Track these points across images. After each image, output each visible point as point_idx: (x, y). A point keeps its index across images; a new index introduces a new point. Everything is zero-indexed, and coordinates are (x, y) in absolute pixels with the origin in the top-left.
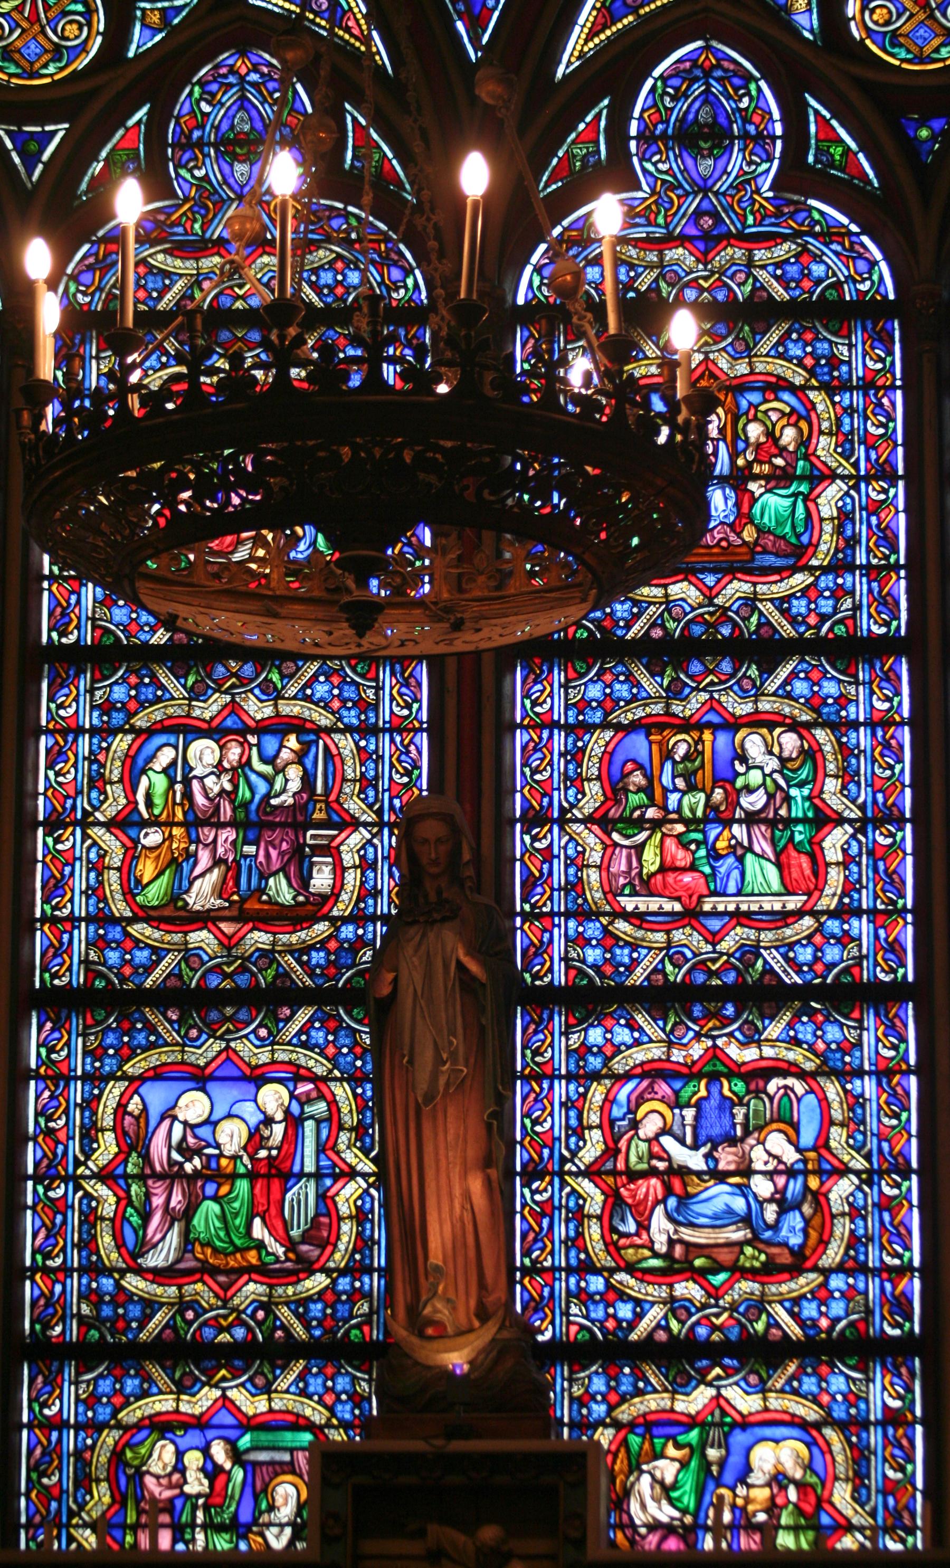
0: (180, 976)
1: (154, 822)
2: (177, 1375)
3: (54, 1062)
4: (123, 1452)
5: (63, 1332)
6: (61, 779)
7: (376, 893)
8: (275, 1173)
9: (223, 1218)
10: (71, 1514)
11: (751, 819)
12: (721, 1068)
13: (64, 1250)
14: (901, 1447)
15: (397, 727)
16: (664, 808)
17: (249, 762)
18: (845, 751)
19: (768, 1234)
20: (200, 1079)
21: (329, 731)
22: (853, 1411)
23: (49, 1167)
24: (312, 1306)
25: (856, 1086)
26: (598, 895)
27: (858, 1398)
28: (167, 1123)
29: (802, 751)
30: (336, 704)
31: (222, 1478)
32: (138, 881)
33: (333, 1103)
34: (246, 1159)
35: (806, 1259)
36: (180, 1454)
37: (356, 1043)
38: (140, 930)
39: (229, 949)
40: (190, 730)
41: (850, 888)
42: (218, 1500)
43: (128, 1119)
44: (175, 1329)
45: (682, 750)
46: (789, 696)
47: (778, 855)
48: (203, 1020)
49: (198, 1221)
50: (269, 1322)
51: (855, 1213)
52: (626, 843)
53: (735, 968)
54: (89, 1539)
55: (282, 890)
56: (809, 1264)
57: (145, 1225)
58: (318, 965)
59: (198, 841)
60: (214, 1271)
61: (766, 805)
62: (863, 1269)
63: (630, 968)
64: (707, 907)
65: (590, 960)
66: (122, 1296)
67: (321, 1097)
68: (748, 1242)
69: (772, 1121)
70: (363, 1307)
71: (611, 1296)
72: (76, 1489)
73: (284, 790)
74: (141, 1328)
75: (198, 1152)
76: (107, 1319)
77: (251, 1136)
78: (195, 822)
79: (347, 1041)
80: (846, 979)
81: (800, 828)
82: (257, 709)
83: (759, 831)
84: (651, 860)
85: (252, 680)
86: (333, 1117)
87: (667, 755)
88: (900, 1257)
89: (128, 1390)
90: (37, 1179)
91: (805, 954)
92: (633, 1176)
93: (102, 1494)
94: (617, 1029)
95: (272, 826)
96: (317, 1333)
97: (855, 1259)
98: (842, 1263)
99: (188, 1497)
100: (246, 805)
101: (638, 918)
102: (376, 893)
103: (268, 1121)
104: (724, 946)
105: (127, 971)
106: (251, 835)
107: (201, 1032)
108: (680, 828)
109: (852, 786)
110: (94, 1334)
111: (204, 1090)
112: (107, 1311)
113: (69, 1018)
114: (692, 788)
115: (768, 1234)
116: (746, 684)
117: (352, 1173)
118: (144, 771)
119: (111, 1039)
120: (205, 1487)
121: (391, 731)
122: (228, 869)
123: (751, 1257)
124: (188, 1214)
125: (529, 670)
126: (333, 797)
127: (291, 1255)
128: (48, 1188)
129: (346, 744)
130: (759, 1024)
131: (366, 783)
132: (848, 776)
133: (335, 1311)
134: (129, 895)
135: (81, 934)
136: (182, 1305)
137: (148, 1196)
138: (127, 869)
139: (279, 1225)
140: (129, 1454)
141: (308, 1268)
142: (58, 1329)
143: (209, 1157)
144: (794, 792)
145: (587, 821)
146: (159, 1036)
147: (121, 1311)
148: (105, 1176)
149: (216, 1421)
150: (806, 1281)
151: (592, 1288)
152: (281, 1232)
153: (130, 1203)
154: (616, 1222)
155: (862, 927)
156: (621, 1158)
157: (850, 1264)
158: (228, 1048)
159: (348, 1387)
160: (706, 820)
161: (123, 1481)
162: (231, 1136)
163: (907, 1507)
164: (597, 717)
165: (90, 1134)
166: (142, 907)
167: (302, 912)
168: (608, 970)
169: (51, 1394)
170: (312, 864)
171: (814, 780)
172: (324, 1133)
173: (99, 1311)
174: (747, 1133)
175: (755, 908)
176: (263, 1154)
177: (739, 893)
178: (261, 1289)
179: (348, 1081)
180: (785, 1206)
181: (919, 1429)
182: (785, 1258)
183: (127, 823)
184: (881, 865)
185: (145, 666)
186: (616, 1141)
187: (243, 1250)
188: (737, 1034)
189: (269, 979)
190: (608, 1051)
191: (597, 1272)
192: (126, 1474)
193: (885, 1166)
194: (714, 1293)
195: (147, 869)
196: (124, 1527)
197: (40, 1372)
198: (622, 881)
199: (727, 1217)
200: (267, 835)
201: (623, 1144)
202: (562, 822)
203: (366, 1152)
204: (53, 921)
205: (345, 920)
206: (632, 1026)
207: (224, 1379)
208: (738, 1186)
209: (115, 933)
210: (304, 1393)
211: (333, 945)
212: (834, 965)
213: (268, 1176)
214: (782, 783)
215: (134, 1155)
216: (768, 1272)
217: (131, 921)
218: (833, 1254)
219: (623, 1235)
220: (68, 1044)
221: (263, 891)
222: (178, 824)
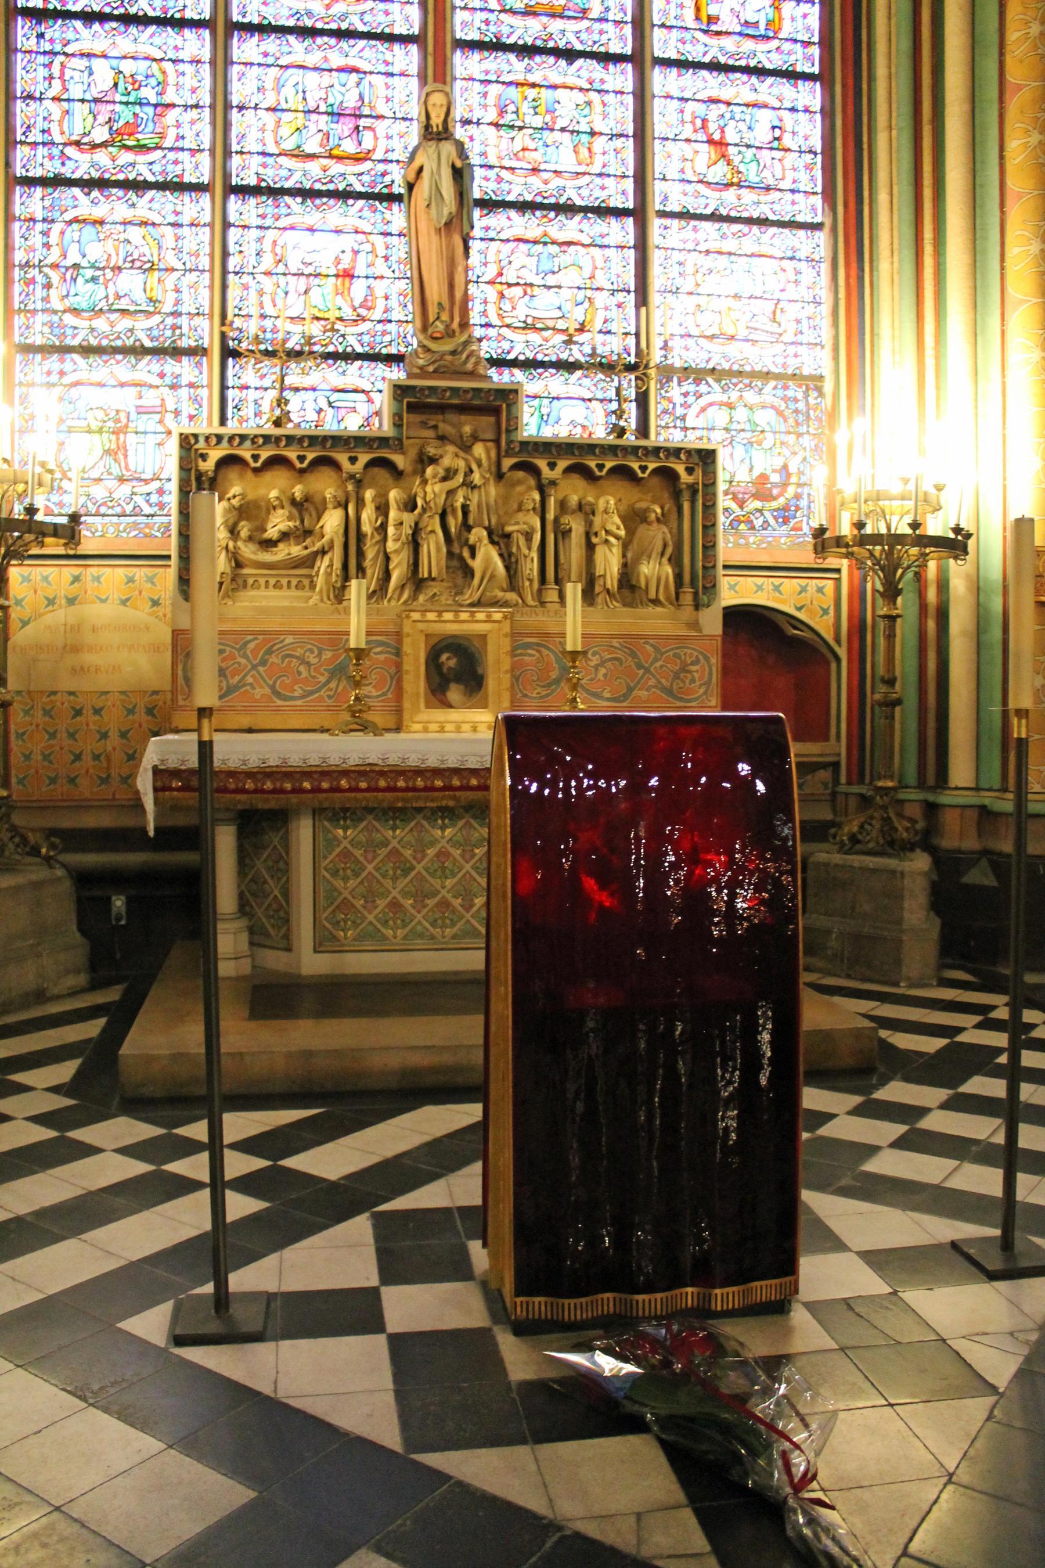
11: (563, 130)
38: (282, 160)
55: (349, 147)
70: (387, 338)
84: (517, 146)
92: (509, 285)
155: (609, 182)
164: (494, 78)
195: (285, 131)
209: (270, 160)
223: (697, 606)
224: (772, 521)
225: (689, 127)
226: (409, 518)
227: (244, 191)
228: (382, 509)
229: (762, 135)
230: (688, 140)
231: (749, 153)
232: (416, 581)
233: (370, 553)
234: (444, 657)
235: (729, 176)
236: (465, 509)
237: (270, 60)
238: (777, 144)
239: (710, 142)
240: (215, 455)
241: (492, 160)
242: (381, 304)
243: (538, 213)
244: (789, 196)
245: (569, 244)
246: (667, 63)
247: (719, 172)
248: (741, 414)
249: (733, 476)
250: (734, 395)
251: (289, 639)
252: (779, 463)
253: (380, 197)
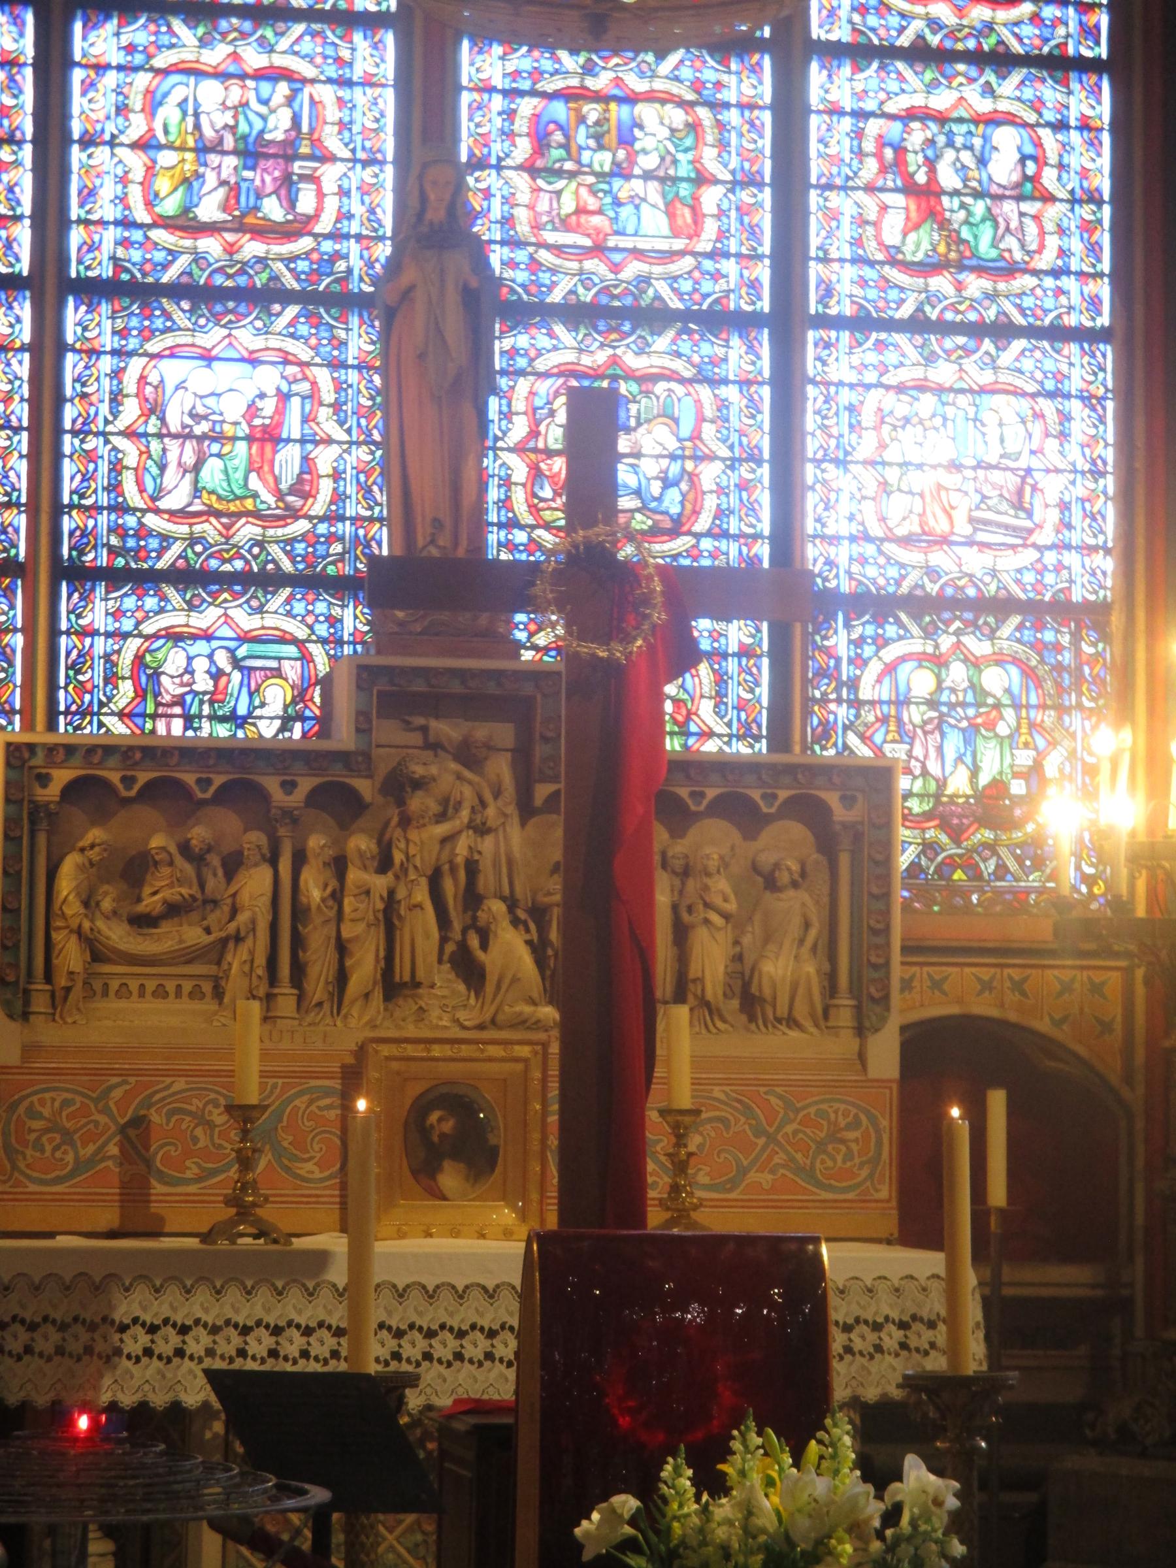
0: (190, 274)
1: (170, 147)
2: (188, 596)
3: (88, 339)
4: (143, 656)
5: (95, 558)
6: (92, 106)
7: (350, 217)
9: (226, 472)
10: (101, 704)
11: (647, 176)
12: (619, 372)
13: (95, 491)
14: (751, 674)
15: (368, 82)
16: (579, 162)
17: (247, 104)
18: (721, 126)
19: (653, 505)
20: (208, 358)
21: (313, 81)
22: (716, 645)
23: (84, 424)
24: (297, 545)
25: (723, 391)
26: (527, 229)
27: (720, 635)
28: (181, 391)
29: (687, 125)
30: (319, 60)
31: (224, 680)
32: (156, 195)
33: (314, 384)
34: (244, 426)
35: (683, 525)
36: (190, 659)
37: (334, 337)
38: (158, 235)
39: (231, 254)
40: (198, 73)
41: (722, 235)
42: (220, 697)
43: (149, 390)
44: (186, 558)
45: (592, 118)
46: (677, 79)
47: (667, 205)
48: (210, 311)
49: (205, 473)
50: (262, 557)
51: (721, 491)
52: (549, 188)
53: (632, 294)
54: (118, 727)
55: (273, 209)
56: (685, 528)
57: (162, 474)
58: (303, 272)
59: (206, 165)
60: (218, 514)
61: (659, 167)
62: (725, 534)
63: (551, 288)
64: (611, 243)
65: (519, 280)
66: (142, 532)
67: (305, 378)
68: (638, 510)
69: (659, 416)
70: (337, 548)
71: (533, 546)
72: (106, 685)
73: (276, 128)
74: (159, 557)
75: (205, 417)
76: (131, 550)
77: (249, 406)
78: (203, 149)
79: (326, 335)
80: (718, 308)
81: (684, 185)
82: (254, 59)
83: (653, 185)
84: (568, 205)
85: (251, 35)
86: (314, 395)
87: (582, 119)
88: (753, 526)
89: (147, 608)
90: (75, 433)
91: (686, 286)
93: (126, 689)
94: (539, 336)
95: (267, 156)
96: (301, 566)
97: (719, 526)
98: (710, 530)
99: (196, 693)
100: (245, 138)
101: (557, 249)
102: (350, 217)
103: (262, 396)
104: (622, 276)
105: (148, 267)
106: (250, 162)
107: (208, 320)
108: (591, 179)
109: (725, 155)
110: (120, 562)
111: (209, 366)
112: (131, 543)
113: (99, 304)
114: (601, 147)
115: (653, 505)
116: (644, 67)
117: (329, 441)
118: (160, 104)
119: (134, 322)
120: (209, 685)
121: (363, 84)
122: (231, 189)
125: (473, 43)
126: (316, 136)
127: (281, 504)
128: (82, 441)
129: (327, 94)
130: (649, 338)
131: (343, 125)
132: (722, 146)
133: (315, 550)
134: (149, 205)
135: (110, 235)
136: (193, 540)
137: (164, 450)
138: (146, 184)
139: (271, 479)
140: (148, 658)
141: (295, 514)
142: (91, 556)
143: (214, 422)
144: (680, 156)
145: (520, 168)
146: (174, 322)
147: (142, 543)
148: (130, 433)
149: (217, 634)
151: (517, 541)
152: (272, 484)
153: (150, 457)
154: (537, 489)
155: (729, 267)
156: (541, 439)
157: (716, 530)
158: (230, 335)
159: (325, 611)
160: (612, 174)
161: (143, 679)
162: (233, 409)
163: (755, 720)
164: (525, 85)
165: (116, 399)
166: (160, 216)
167: (289, 228)
168: (533, 289)
169: (85, 607)
170: (298, 190)
171: (696, 148)
172: (308, 408)
173: (124, 542)
174: (639, 424)
175: (647, 246)
176: (257, 422)
177: (635, 235)
178: (259, 530)
179: (327, 366)
180: (667, 483)
181: (765, 662)
182: (668, 524)
183: (143, 145)
184: (746, 219)
185: (162, 17)
186: (538, 426)
187: (242, 498)
188: (633, 346)
189: (264, 281)
190: (533, 353)
191: (522, 527)
192: (146, 675)
193: (744, 456)
195: (163, 184)
196: (144, 715)
197: (76, 590)
198: (545, 219)
200: (262, 164)
201: (542, 428)
202: (499, 168)
203: (341, 423)
204: (86, 223)
205: (326, 237)
206: (551, 335)
207: (225, 601)
208: (632, 465)
209: (137, 235)
210: (289, 614)
211: (315, 256)
212: (708, 295)
213: (262, 441)
214: (672, 149)
215: (153, 417)
217: (150, 227)
218: (703, 523)
219: (542, 500)
220: (99, 324)
221: (257, 208)
222: (190, 150)
223: (860, 1031)
224: (1012, 864)
225: (872, 164)
226: (380, 883)
227: (92, 290)
228: (339, 865)
229: (1003, 169)
230: (870, 188)
231: (979, 208)
232: (393, 986)
233: (318, 940)
234: (434, 1117)
235: (942, 249)
236: (472, 868)
237: (139, 59)
238: (1029, 188)
239: (910, 188)
240: (62, 777)
241: (523, 229)
242: (326, 487)
243: (602, 325)
244: (1049, 282)
245: (654, 378)
246: (834, 51)
247: (921, 244)
248: (957, 673)
249: (942, 784)
250: (946, 642)
251: (180, 1084)
252: (1024, 758)
253: (327, 299)
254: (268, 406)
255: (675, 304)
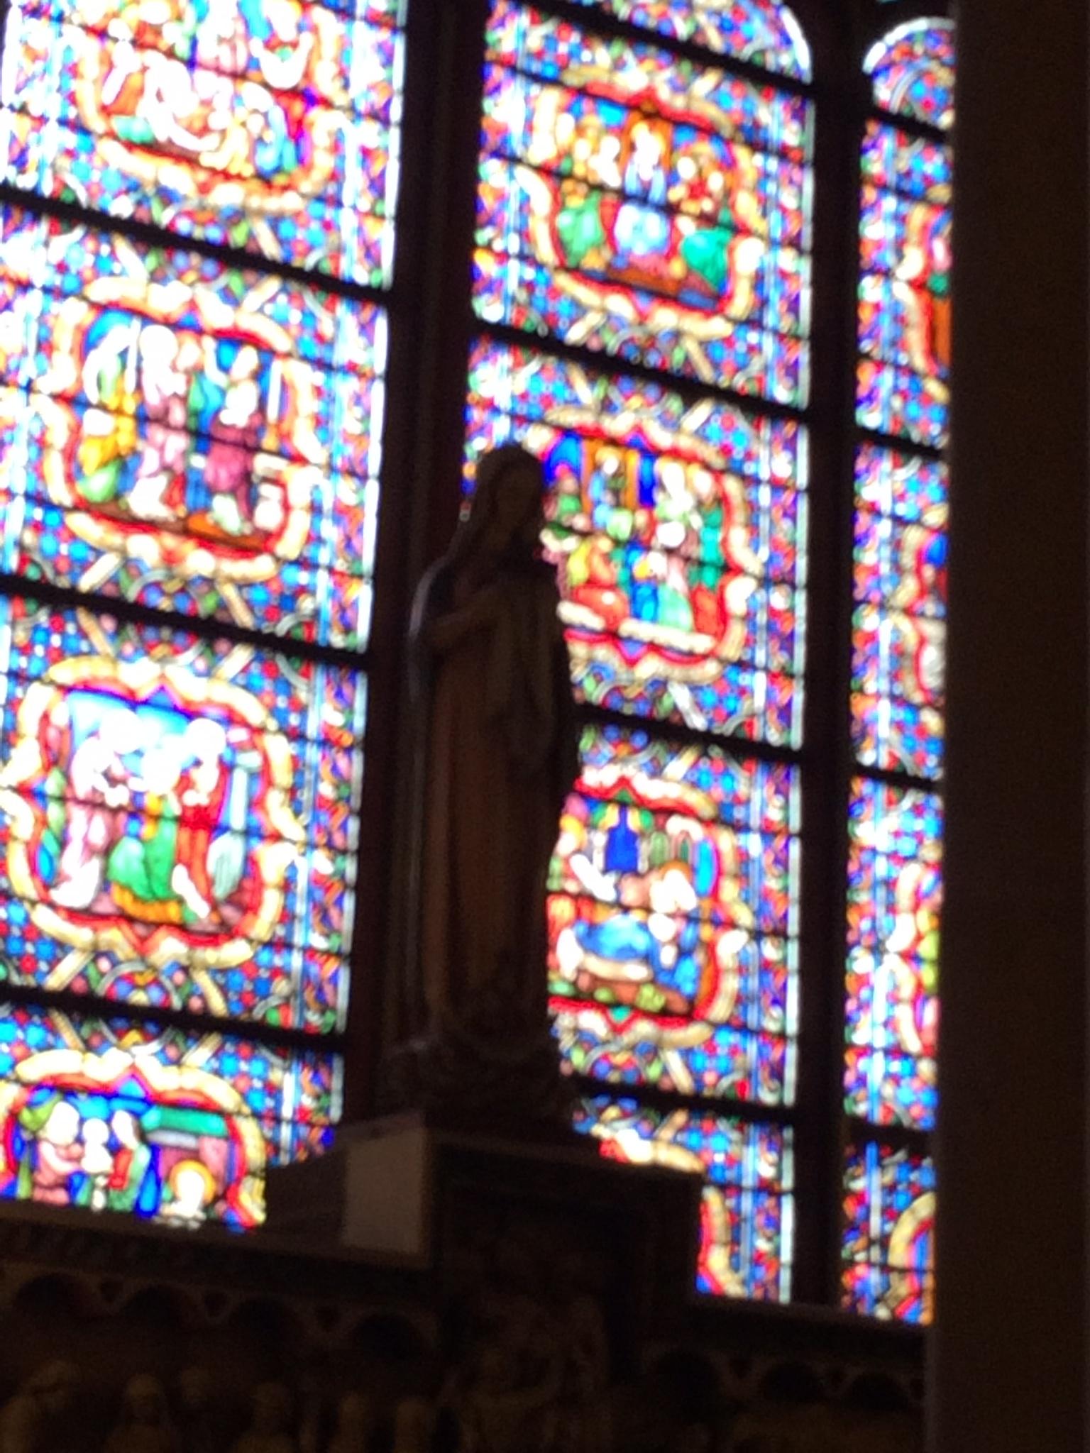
8: (203, 822)
11: (670, 552)
38: (80, 523)
123: (651, 999)
124: (107, 852)
136: (97, 953)
150: (695, 1033)
174: (651, 868)
194: (617, 1029)
195: (89, 454)
199: (627, 953)
209: (53, 519)
216: (664, 1016)
254: (206, 779)
255: (697, 722)
